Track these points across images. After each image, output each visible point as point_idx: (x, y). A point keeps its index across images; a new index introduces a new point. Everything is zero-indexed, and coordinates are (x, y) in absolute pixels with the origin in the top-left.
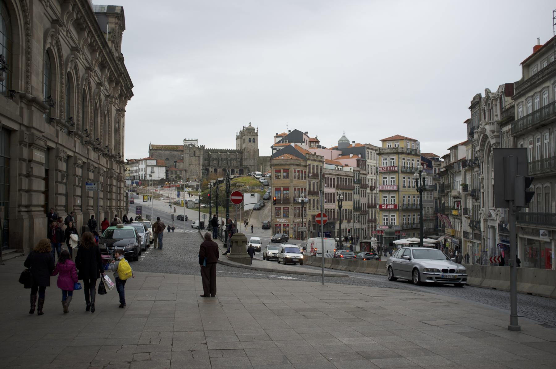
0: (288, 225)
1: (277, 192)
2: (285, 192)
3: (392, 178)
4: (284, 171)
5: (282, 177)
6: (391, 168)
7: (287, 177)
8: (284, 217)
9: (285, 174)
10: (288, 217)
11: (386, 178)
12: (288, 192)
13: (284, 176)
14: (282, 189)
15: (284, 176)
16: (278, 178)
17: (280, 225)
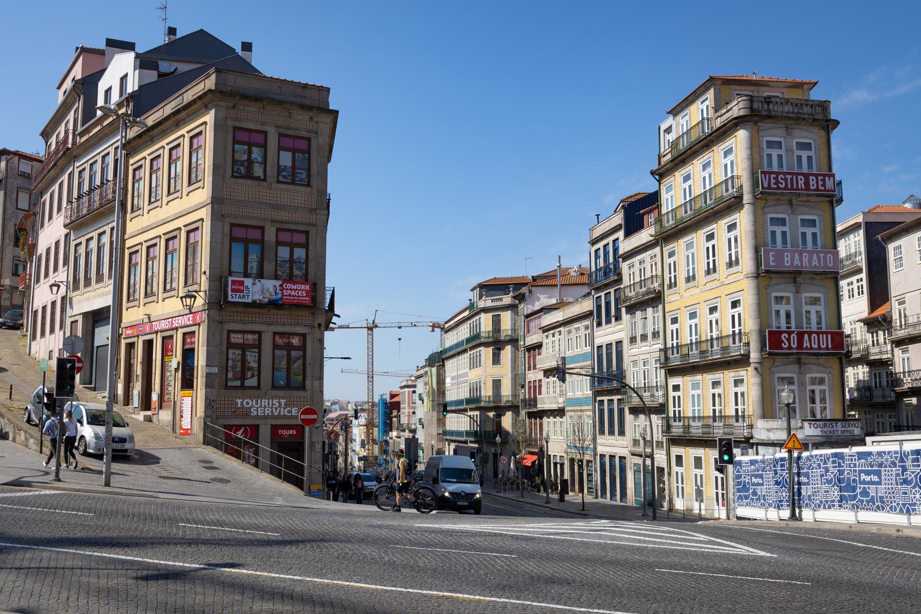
0: (300, 429)
1: (238, 249)
2: (284, 253)
3: (805, 223)
4: (288, 141)
5: (272, 171)
6: (812, 181)
7: (291, 177)
8: (274, 387)
9: (286, 159)
10: (303, 387)
11: (782, 222)
12: (300, 253)
13: (280, 170)
14: (270, 235)
15: (280, 170)
16: (249, 176)
17: (253, 431)
